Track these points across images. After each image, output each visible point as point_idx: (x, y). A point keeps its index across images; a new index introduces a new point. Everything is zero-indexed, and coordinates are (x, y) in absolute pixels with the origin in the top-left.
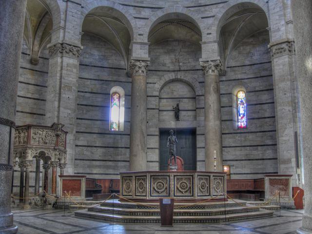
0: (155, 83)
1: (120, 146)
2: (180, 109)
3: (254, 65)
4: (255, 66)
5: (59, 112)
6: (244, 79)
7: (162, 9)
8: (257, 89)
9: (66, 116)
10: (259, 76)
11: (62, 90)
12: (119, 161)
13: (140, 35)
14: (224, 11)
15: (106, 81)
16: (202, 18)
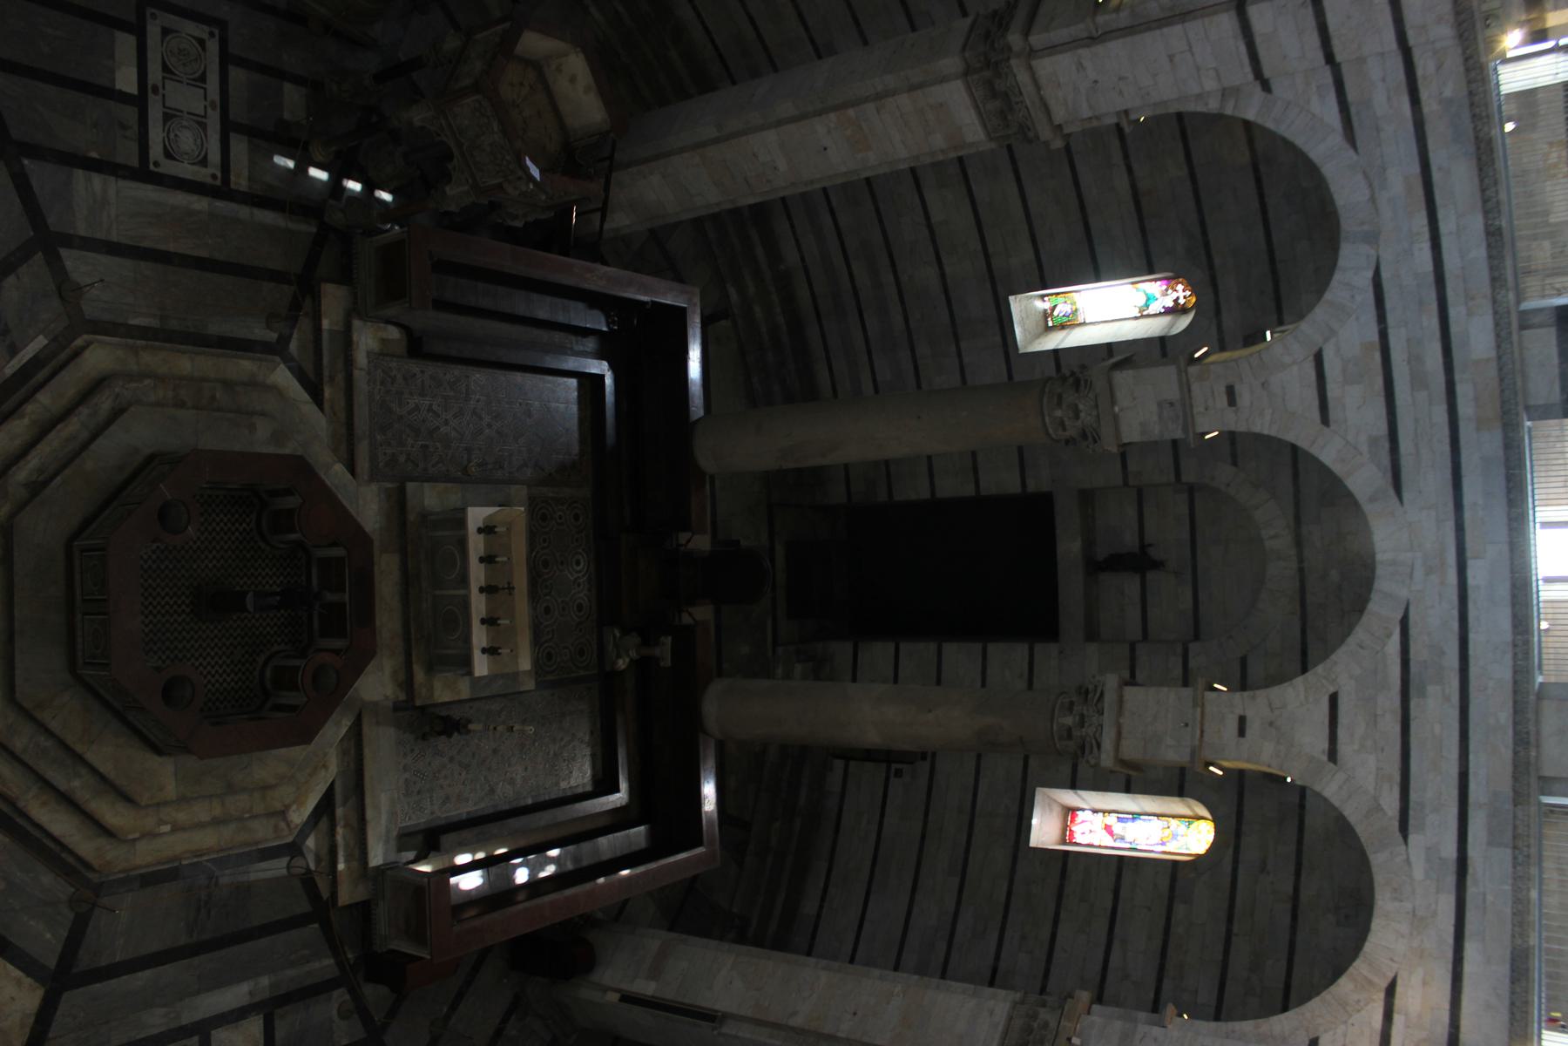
0: (1235, 464)
1: (963, 345)
2: (1150, 575)
3: (1294, 917)
4: (1287, 920)
5: (762, 128)
6: (1236, 862)
7: (1392, 492)
8: (1180, 910)
10: (1235, 929)
11: (832, 116)
12: (913, 350)
13: (1231, 393)
14: (1352, 813)
15: (1207, 245)
16: (1334, 700)
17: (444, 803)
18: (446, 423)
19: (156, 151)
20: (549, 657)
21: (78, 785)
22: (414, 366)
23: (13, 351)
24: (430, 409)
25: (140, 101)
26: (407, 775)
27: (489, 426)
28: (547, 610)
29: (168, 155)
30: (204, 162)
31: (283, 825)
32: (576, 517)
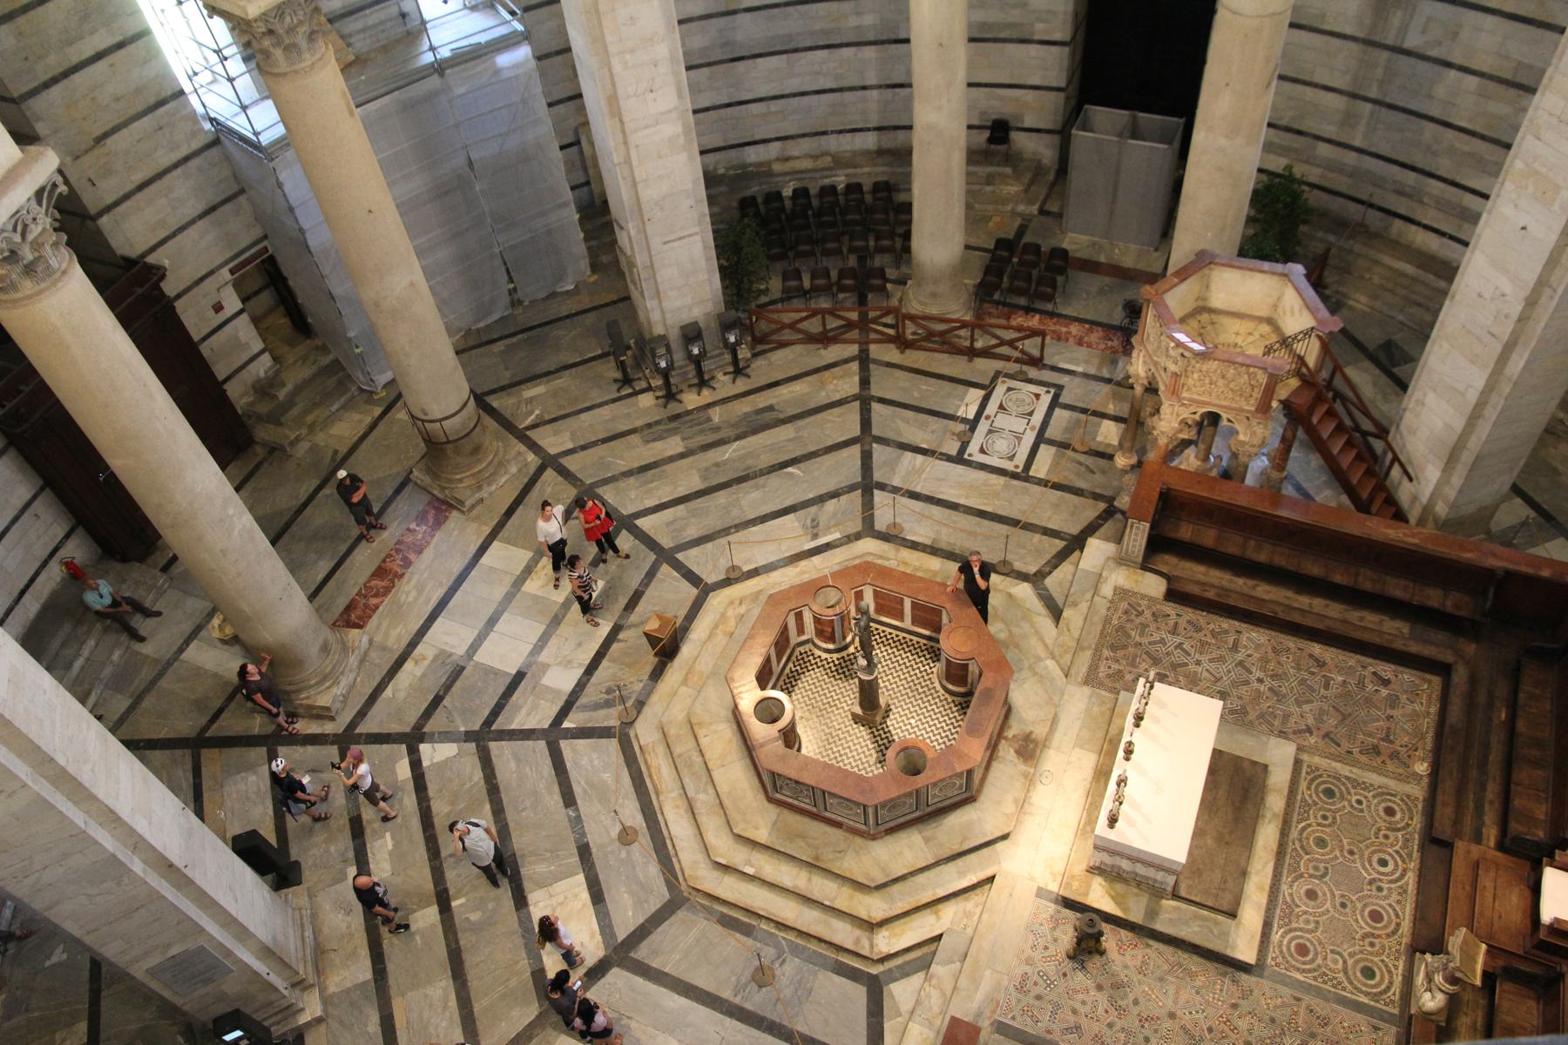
9: (1487, 295)
17: (1069, 1030)
18: (1198, 663)
19: (973, 448)
20: (1302, 950)
21: (703, 799)
22: (1171, 609)
23: (815, 536)
24: (1180, 646)
25: (973, 424)
26: (1028, 969)
27: (1260, 681)
28: (1311, 895)
29: (982, 451)
30: (1011, 458)
31: (866, 943)
32: (1390, 812)
